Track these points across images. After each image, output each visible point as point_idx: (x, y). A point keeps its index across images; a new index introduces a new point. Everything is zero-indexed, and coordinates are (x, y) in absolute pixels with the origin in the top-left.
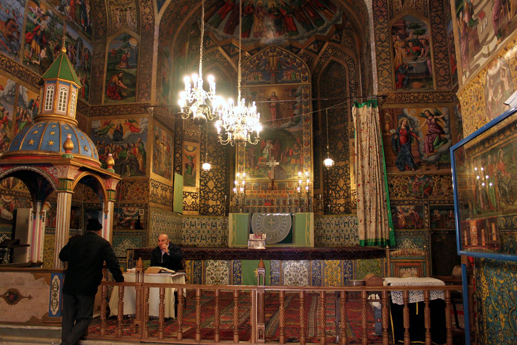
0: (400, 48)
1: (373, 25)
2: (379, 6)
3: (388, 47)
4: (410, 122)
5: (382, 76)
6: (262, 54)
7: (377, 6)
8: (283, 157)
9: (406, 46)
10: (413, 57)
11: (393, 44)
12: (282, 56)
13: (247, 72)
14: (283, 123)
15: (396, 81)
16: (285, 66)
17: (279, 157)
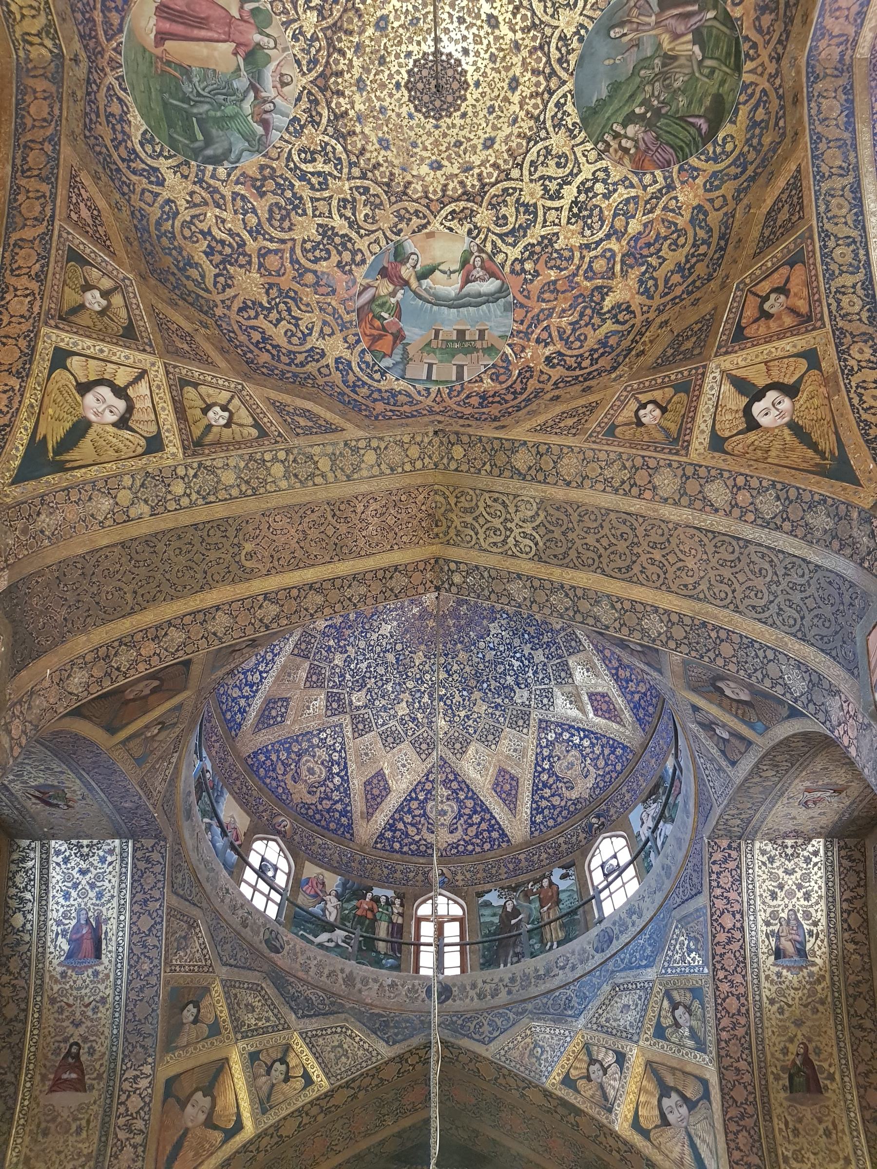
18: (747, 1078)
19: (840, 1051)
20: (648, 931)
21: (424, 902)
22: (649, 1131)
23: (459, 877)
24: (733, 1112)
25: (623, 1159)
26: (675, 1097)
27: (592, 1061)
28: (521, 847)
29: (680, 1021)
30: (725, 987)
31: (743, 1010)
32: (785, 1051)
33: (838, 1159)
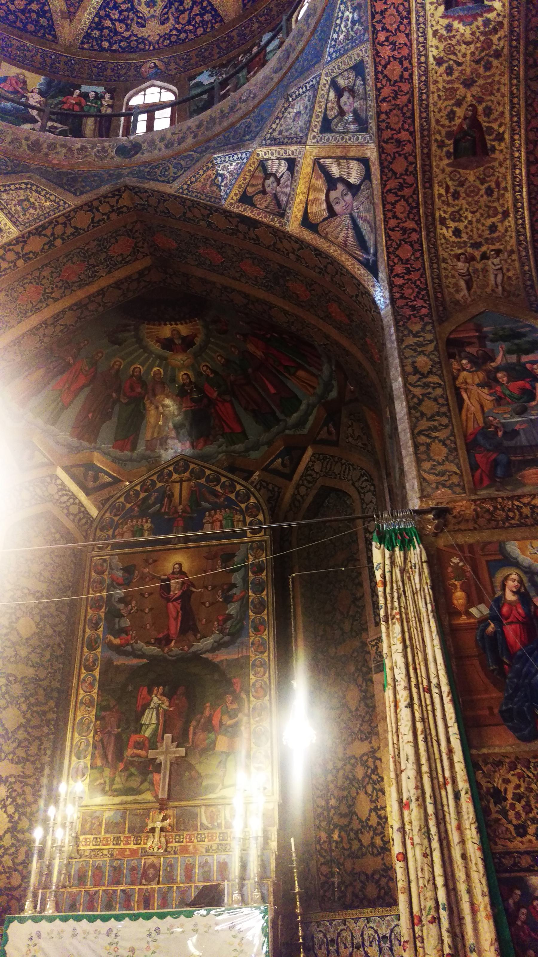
0: (474, 389)
1: (394, 338)
2: (406, 295)
3: (440, 385)
4: (531, 580)
5: (430, 459)
6: (155, 478)
7: (402, 297)
8: (195, 734)
9: (490, 382)
10: (514, 406)
11: (455, 378)
12: (203, 481)
13: (116, 519)
14: (198, 640)
15: (474, 467)
16: (207, 501)
17: (185, 732)
18: (408, 148)
19: (512, 108)
20: (319, 29)
21: (136, 94)
22: (317, 225)
23: (173, 66)
24: (392, 184)
25: (299, 258)
26: (341, 187)
27: (267, 175)
28: (233, 22)
29: (345, 108)
30: (386, 52)
31: (406, 75)
32: (451, 116)
33: (495, 215)
